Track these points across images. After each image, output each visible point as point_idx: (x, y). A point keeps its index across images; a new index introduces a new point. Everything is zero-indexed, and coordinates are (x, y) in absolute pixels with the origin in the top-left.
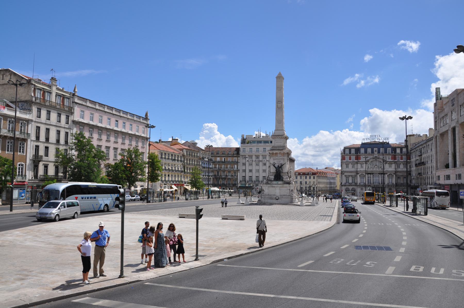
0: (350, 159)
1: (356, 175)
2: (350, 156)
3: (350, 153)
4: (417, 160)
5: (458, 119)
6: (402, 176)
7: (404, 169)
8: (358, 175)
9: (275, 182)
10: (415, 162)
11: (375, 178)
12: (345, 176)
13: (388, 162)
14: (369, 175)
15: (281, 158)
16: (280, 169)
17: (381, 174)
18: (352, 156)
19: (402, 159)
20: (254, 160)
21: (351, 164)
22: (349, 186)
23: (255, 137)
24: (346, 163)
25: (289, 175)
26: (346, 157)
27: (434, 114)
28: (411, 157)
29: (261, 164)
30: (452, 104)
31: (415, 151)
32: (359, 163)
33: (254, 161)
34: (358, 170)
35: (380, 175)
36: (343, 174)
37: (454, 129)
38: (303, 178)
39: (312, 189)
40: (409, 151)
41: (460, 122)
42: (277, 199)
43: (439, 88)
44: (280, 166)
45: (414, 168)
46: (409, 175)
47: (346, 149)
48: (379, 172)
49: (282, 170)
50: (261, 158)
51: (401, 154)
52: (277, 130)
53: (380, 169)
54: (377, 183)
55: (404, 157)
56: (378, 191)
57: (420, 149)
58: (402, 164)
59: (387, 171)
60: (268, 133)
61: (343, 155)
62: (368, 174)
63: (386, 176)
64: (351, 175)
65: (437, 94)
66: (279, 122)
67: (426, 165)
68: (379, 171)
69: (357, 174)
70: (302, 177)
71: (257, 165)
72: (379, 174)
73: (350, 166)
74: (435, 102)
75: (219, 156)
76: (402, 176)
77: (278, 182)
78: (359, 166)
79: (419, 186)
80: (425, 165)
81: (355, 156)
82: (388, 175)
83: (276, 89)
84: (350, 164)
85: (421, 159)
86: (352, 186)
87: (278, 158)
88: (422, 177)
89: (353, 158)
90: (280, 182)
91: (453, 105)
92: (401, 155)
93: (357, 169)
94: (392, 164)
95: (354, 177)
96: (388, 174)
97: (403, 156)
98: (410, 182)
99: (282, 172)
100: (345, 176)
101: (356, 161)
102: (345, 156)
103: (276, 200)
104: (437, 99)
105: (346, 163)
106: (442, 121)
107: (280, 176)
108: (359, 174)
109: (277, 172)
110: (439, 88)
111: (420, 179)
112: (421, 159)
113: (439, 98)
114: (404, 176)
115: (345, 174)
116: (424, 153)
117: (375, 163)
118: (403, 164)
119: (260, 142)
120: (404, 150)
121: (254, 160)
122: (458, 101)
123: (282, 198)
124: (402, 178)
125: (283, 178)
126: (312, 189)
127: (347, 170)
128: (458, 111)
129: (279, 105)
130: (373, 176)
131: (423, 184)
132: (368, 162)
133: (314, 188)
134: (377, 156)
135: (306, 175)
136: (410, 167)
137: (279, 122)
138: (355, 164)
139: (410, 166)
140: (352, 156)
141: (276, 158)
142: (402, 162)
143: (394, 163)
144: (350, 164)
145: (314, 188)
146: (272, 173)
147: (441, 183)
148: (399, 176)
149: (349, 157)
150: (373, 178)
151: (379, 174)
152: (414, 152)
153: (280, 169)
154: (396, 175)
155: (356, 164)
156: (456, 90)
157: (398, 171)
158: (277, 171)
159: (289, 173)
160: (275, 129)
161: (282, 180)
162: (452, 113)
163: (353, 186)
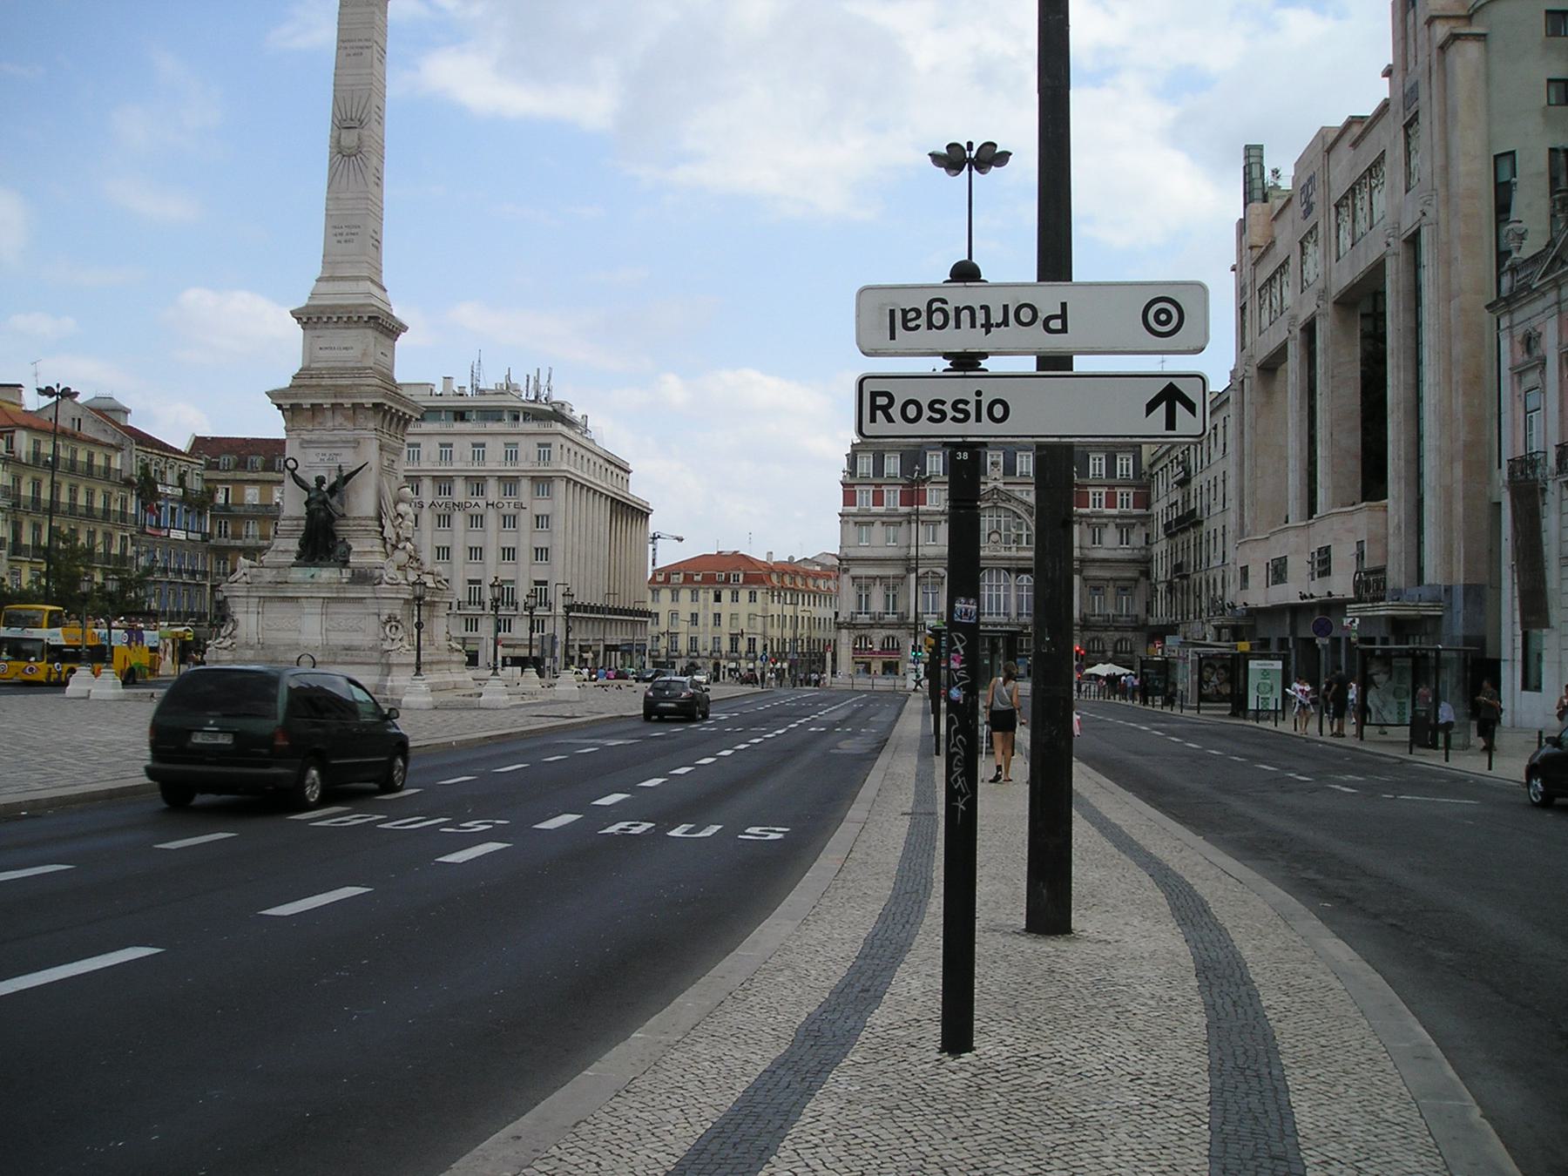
0: (878, 500)
1: (903, 578)
2: (880, 485)
3: (879, 468)
4: (1171, 506)
5: (1327, 273)
6: (1111, 583)
7: (1121, 551)
9: (298, 574)
10: (1167, 514)
12: (854, 578)
16: (334, 501)
18: (885, 488)
19: (1111, 503)
20: (427, 501)
21: (883, 523)
22: (871, 626)
23: (441, 395)
24: (859, 519)
25: (389, 532)
26: (857, 488)
27: (1236, 276)
28: (1154, 497)
29: (459, 518)
30: (1305, 207)
31: (1166, 466)
33: (426, 506)
35: (1013, 576)
36: (846, 571)
37: (1309, 329)
38: (706, 600)
39: (743, 645)
40: (1145, 466)
41: (1334, 292)
43: (1261, 148)
44: (331, 479)
45: (1161, 547)
46: (1142, 579)
48: (1006, 564)
49: (343, 505)
50: (460, 491)
51: (1112, 481)
52: (332, 279)
53: (1014, 549)
54: (998, 614)
55: (1126, 494)
57: (1183, 453)
58: (1112, 527)
60: (518, 380)
61: (849, 481)
64: (881, 578)
65: (1250, 173)
66: (348, 230)
67: (1205, 523)
68: (1009, 559)
70: (701, 592)
71: (444, 520)
72: (1008, 570)
74: (1242, 217)
75: (255, 482)
76: (1111, 583)
77: (313, 570)
79: (1178, 625)
80: (1201, 523)
81: (899, 488)
83: (338, 49)
84: (878, 525)
85: (1186, 501)
86: (882, 627)
87: (327, 436)
88: (1188, 587)
89: (892, 498)
90: (327, 574)
91: (1308, 211)
92: (1110, 487)
95: (893, 586)
97: (1118, 491)
98: (1147, 611)
99: (344, 515)
100: (854, 578)
101: (906, 509)
102: (853, 485)
104: (1248, 198)
105: (859, 519)
106: (1267, 302)
107: (334, 537)
109: (311, 514)
110: (1261, 148)
111: (1182, 595)
112: (1189, 500)
113: (1258, 194)
114: (1119, 583)
115: (857, 571)
116: (1199, 470)
118: (1117, 526)
119: (460, 415)
120: (1124, 463)
121: (427, 501)
122: (1327, 184)
123: (334, 663)
124: (1111, 590)
125: (349, 548)
126: (743, 645)
128: (1327, 238)
129: (349, 139)
131: (1191, 616)
133: (752, 642)
134: (1001, 486)
135: (719, 586)
136: (1147, 543)
137: (345, 231)
138: (901, 523)
139: (1147, 535)
140: (885, 488)
141: (314, 436)
142: (1114, 517)
144: (878, 525)
145: (752, 642)
146: (291, 518)
147: (1252, 603)
148: (1097, 583)
149: (872, 488)
151: (1008, 570)
152: (1162, 469)
153: (334, 501)
154: (1085, 580)
155: (905, 525)
156: (1323, 132)
157: (1094, 561)
158: (313, 506)
159: (387, 522)
160: (317, 271)
161: (345, 564)
162: (1303, 253)
163: (890, 626)
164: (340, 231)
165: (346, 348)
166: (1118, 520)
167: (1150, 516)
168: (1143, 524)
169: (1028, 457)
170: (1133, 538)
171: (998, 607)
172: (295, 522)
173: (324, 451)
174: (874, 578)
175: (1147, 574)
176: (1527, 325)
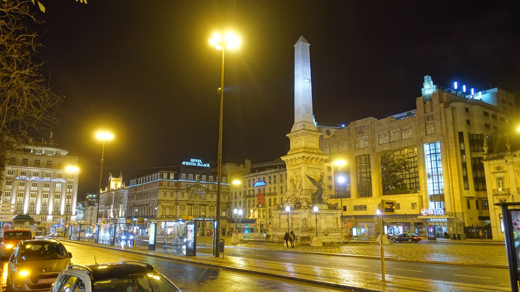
4: (249, 191)
8: (178, 206)
11: (197, 210)
13: (210, 192)
14: (189, 206)
15: (317, 166)
17: (203, 205)
21: (170, 192)
26: (164, 182)
32: (179, 192)
34: (179, 199)
36: (160, 204)
42: (326, 235)
47: (164, 173)
53: (202, 199)
56: (198, 225)
59: (209, 202)
62: (189, 205)
63: (207, 207)
66: (308, 110)
69: (177, 204)
73: (168, 194)
78: (179, 194)
79: (256, 219)
81: (174, 183)
82: (209, 207)
93: (177, 198)
94: (214, 194)
96: (210, 205)
98: (229, 215)
101: (176, 188)
103: (326, 237)
108: (179, 204)
117: (196, 193)
127: (165, 198)
130: (194, 207)
132: (190, 190)
138: (174, 192)
139: (229, 197)
140: (170, 183)
143: (215, 193)
150: (194, 210)
155: (175, 193)
164: (307, 109)
165: (314, 143)
166: (223, 193)
167: (229, 192)
168: (228, 195)
169: (205, 177)
170: (226, 197)
171: (195, 214)
172: (308, 191)
173: (313, 171)
174: (167, 206)
175: (228, 206)
176: (497, 165)
